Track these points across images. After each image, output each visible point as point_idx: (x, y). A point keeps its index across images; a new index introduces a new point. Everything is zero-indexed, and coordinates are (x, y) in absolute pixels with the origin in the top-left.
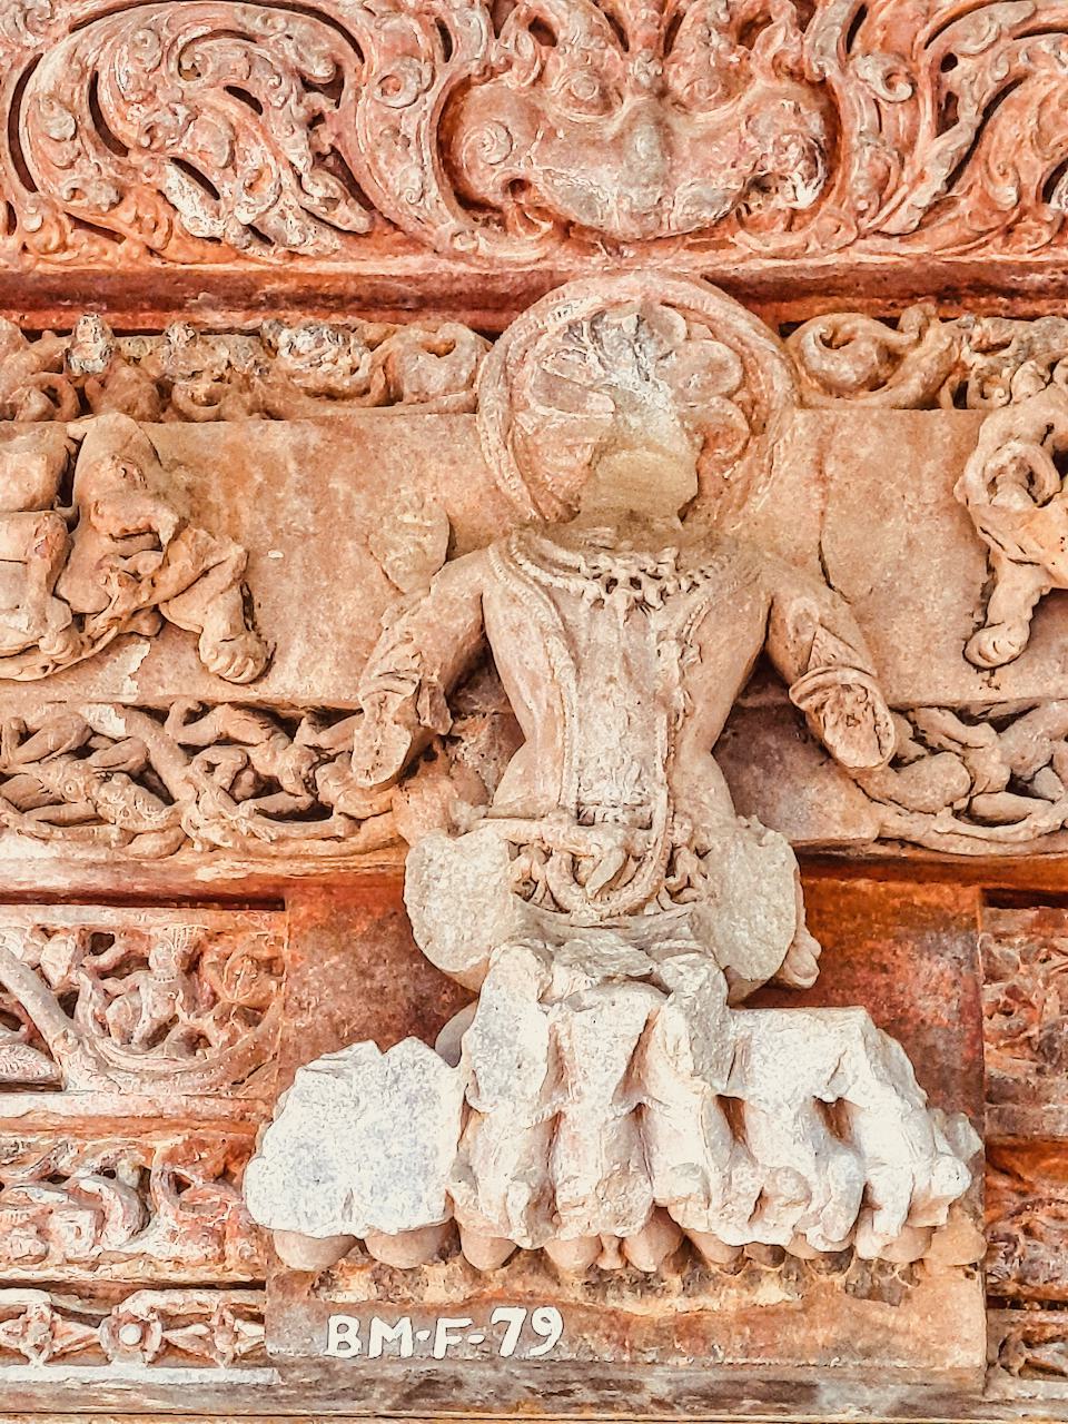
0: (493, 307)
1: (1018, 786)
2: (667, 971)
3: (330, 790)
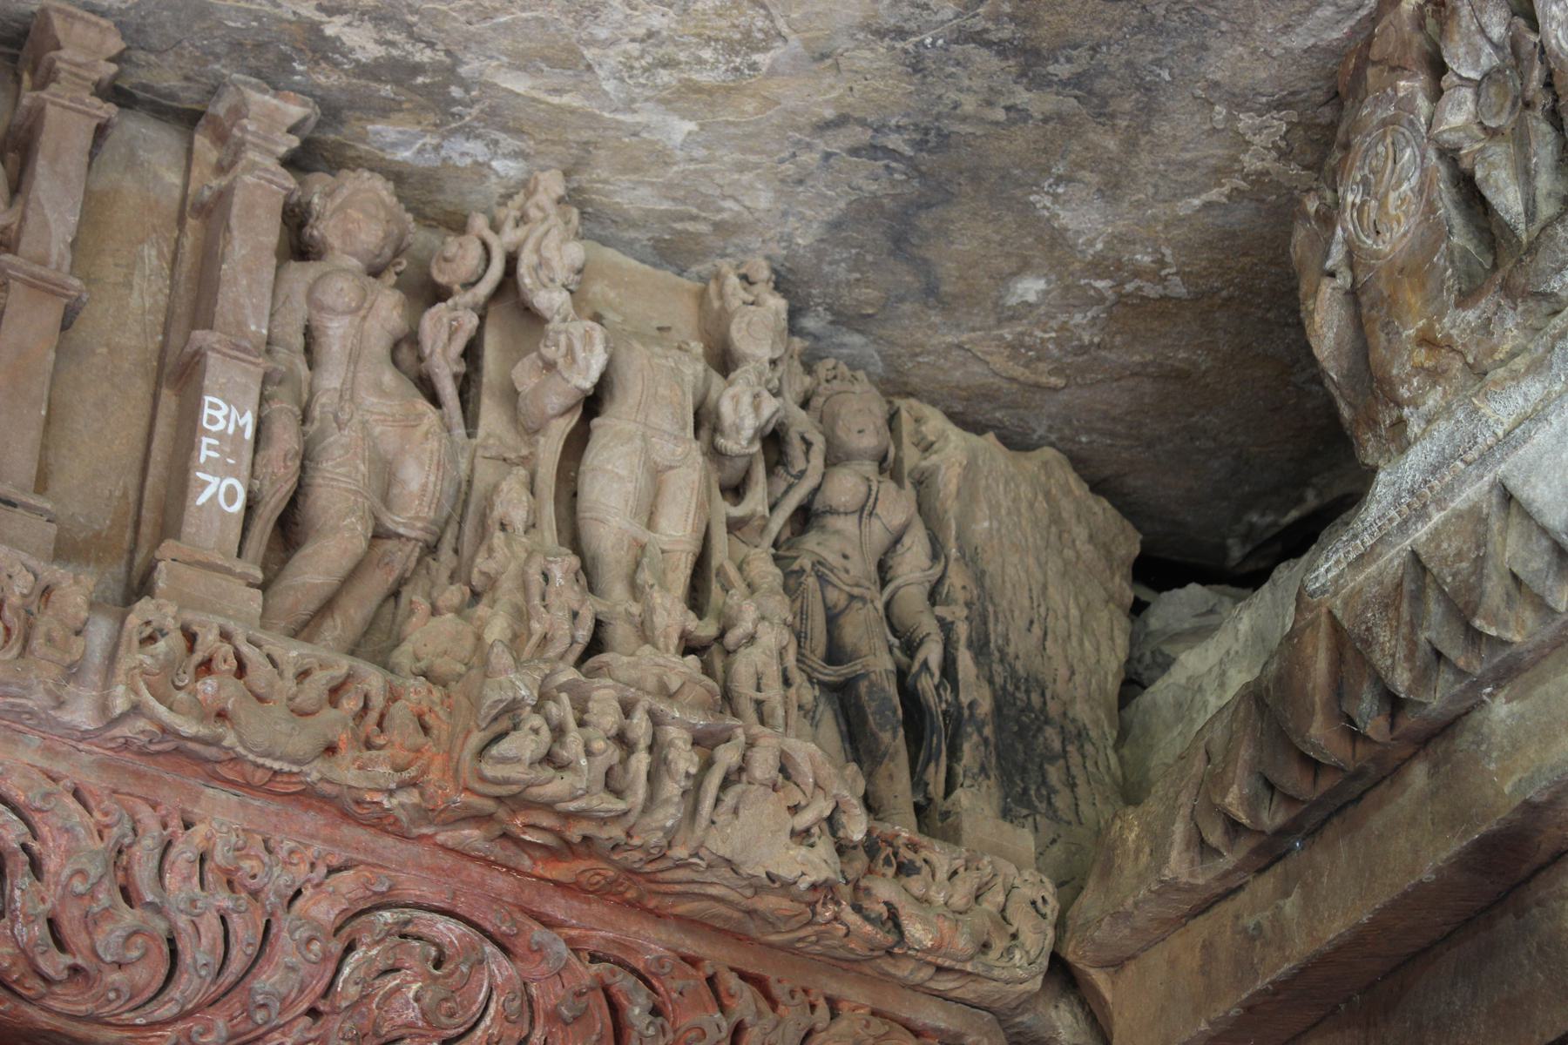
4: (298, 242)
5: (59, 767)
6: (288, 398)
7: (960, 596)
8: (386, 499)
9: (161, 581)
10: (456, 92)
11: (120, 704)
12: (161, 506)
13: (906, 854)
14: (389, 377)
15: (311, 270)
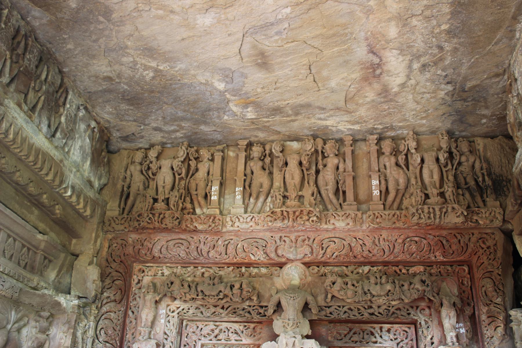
0: (281, 265)
1: (331, 313)
2: (296, 336)
3: (266, 313)
5: (364, 233)
7: (485, 168)
11: (368, 226)
13: (478, 212)
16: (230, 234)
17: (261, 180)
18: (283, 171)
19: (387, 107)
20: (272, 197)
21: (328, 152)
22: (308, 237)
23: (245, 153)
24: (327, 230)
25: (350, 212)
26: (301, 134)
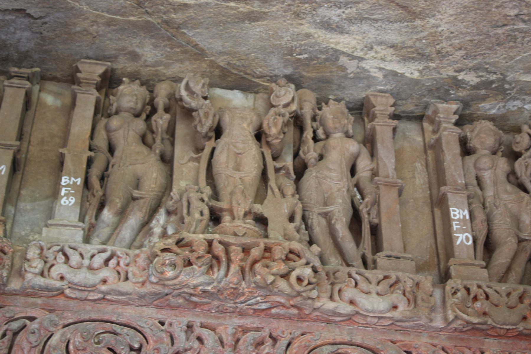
4: (466, 150)
5: (436, 342)
6: (477, 203)
8: (519, 229)
9: (453, 272)
10: (507, 86)
11: (451, 317)
12: (445, 248)
14: (509, 187)
15: (473, 158)
16: (31, 300)
17: (139, 168)
18: (207, 152)
19: (516, 12)
20: (169, 213)
21: (330, 124)
22: (271, 336)
23: (97, 94)
24: (329, 319)
25: (400, 274)
26: (259, 71)
